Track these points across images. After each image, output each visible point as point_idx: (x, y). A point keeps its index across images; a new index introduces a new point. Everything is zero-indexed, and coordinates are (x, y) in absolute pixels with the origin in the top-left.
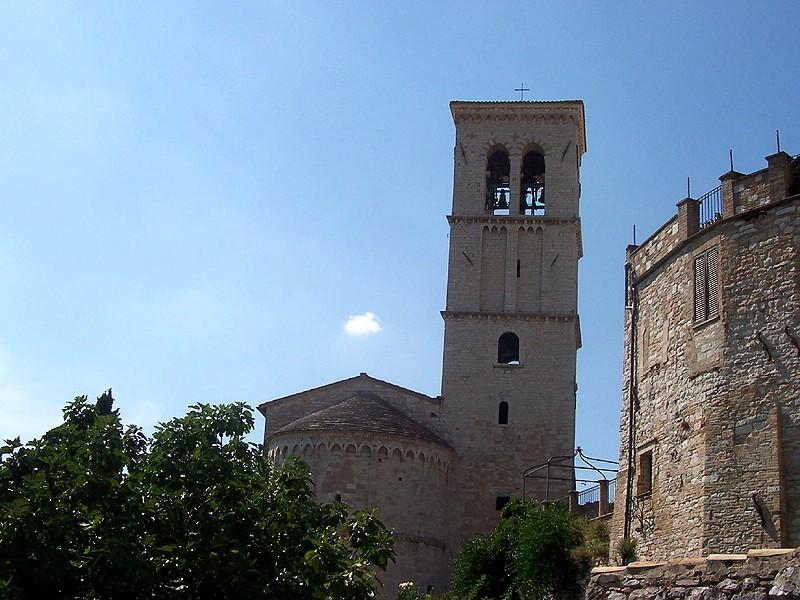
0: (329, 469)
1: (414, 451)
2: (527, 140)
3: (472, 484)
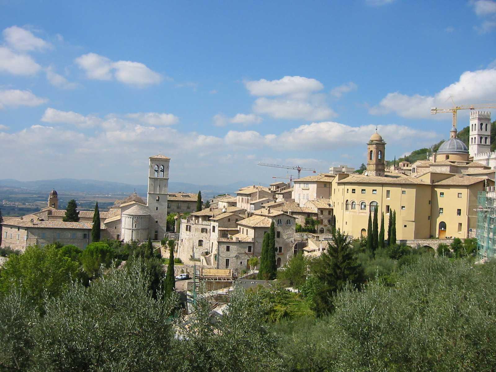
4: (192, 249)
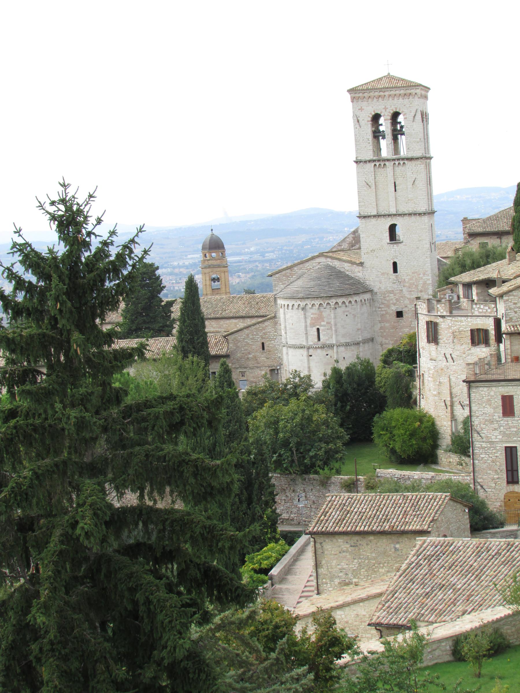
0: (312, 316)
1: (352, 300)
2: (392, 110)
3: (383, 306)
4: (449, 408)
